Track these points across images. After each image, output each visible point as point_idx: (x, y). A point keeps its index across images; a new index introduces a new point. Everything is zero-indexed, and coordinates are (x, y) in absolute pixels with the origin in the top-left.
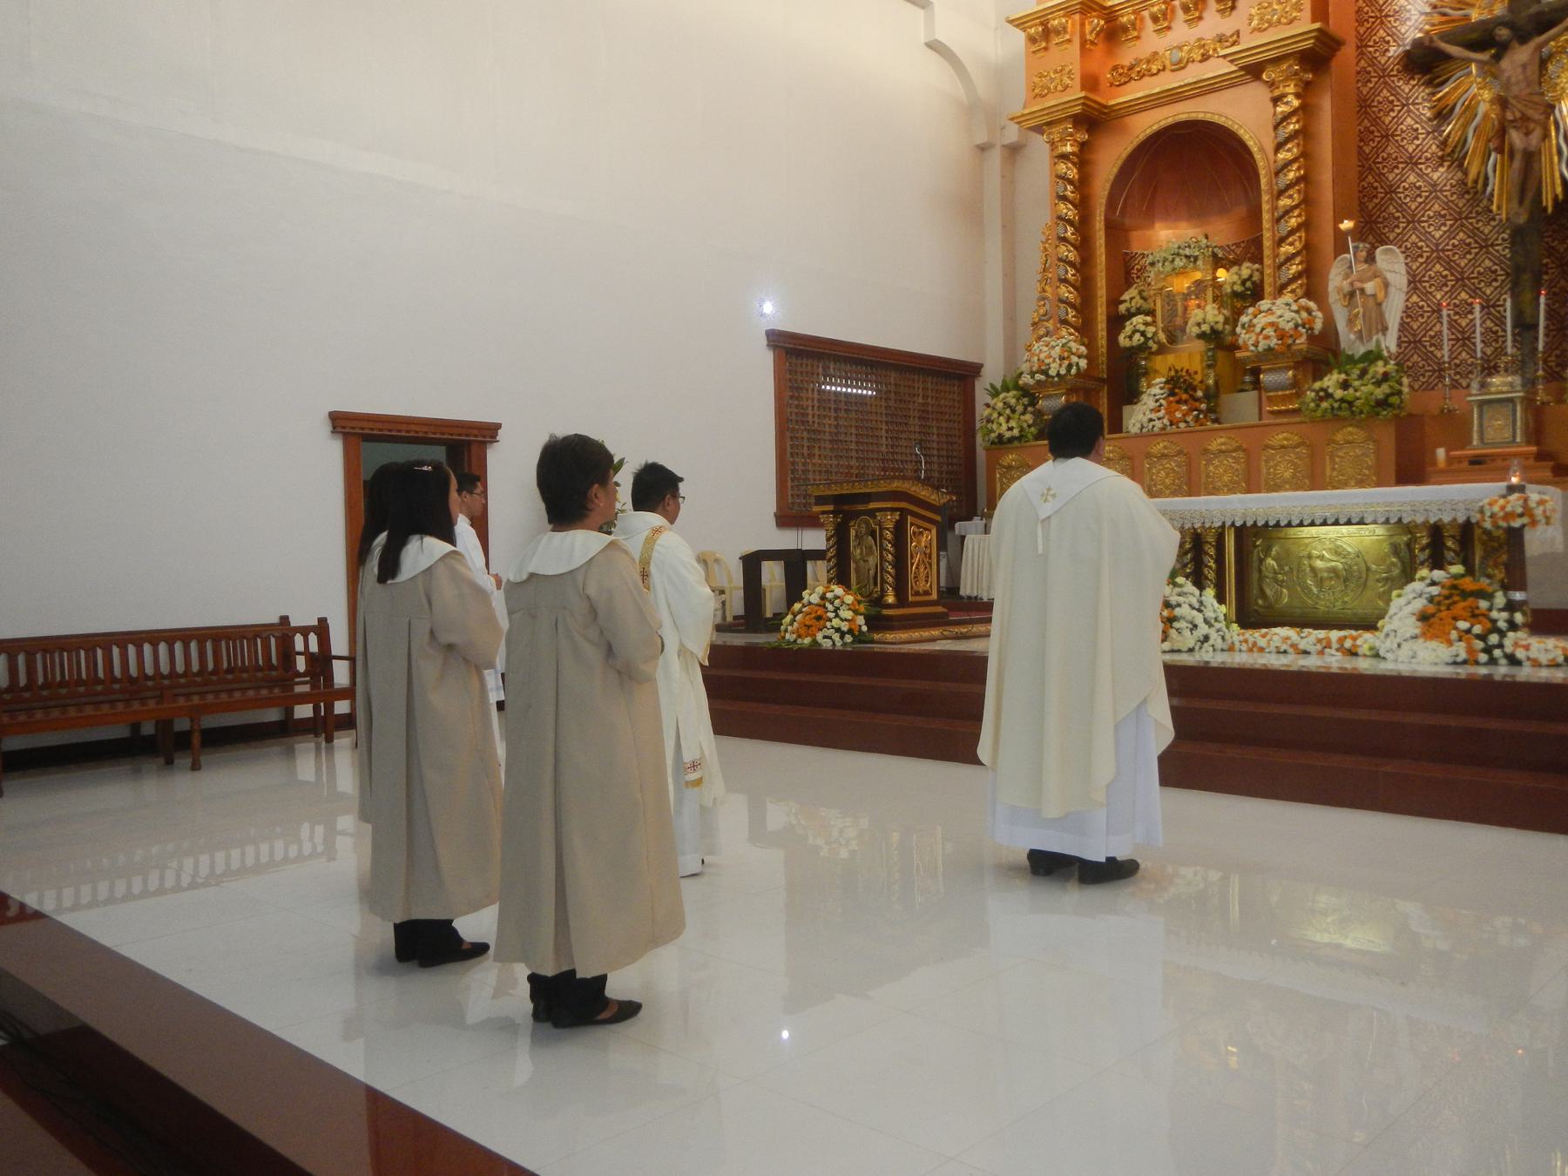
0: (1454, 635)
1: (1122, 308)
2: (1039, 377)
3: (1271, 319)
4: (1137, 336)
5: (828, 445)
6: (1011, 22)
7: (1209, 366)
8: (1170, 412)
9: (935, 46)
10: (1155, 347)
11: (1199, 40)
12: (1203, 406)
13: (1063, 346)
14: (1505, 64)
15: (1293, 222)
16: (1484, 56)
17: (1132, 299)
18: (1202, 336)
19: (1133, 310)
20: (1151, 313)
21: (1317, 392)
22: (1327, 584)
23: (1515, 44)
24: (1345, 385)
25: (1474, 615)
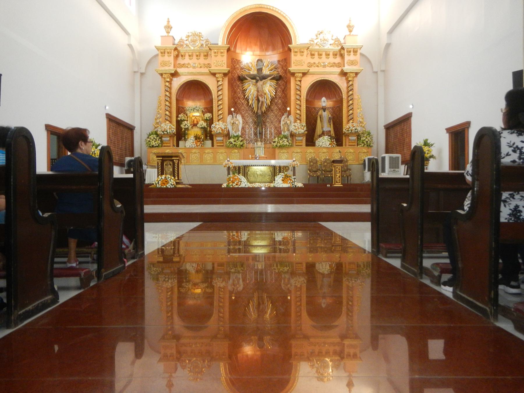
0: (289, 183)
1: (179, 119)
2: (165, 132)
3: (220, 126)
4: (186, 126)
5: (113, 144)
6: (156, 47)
7: (202, 134)
8: (196, 143)
9: (130, 46)
10: (190, 129)
11: (200, 64)
12: (203, 143)
13: (170, 126)
14: (258, 84)
15: (221, 107)
16: (254, 81)
17: (182, 117)
18: (202, 128)
19: (182, 119)
20: (187, 121)
21: (229, 142)
22: (259, 176)
23: (260, 81)
24: (235, 141)
25: (290, 180)
